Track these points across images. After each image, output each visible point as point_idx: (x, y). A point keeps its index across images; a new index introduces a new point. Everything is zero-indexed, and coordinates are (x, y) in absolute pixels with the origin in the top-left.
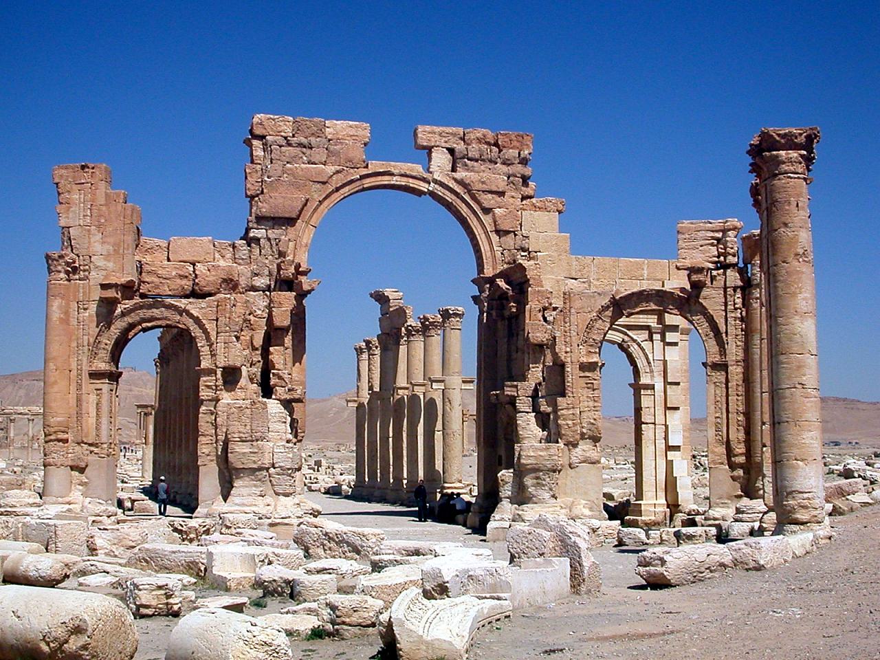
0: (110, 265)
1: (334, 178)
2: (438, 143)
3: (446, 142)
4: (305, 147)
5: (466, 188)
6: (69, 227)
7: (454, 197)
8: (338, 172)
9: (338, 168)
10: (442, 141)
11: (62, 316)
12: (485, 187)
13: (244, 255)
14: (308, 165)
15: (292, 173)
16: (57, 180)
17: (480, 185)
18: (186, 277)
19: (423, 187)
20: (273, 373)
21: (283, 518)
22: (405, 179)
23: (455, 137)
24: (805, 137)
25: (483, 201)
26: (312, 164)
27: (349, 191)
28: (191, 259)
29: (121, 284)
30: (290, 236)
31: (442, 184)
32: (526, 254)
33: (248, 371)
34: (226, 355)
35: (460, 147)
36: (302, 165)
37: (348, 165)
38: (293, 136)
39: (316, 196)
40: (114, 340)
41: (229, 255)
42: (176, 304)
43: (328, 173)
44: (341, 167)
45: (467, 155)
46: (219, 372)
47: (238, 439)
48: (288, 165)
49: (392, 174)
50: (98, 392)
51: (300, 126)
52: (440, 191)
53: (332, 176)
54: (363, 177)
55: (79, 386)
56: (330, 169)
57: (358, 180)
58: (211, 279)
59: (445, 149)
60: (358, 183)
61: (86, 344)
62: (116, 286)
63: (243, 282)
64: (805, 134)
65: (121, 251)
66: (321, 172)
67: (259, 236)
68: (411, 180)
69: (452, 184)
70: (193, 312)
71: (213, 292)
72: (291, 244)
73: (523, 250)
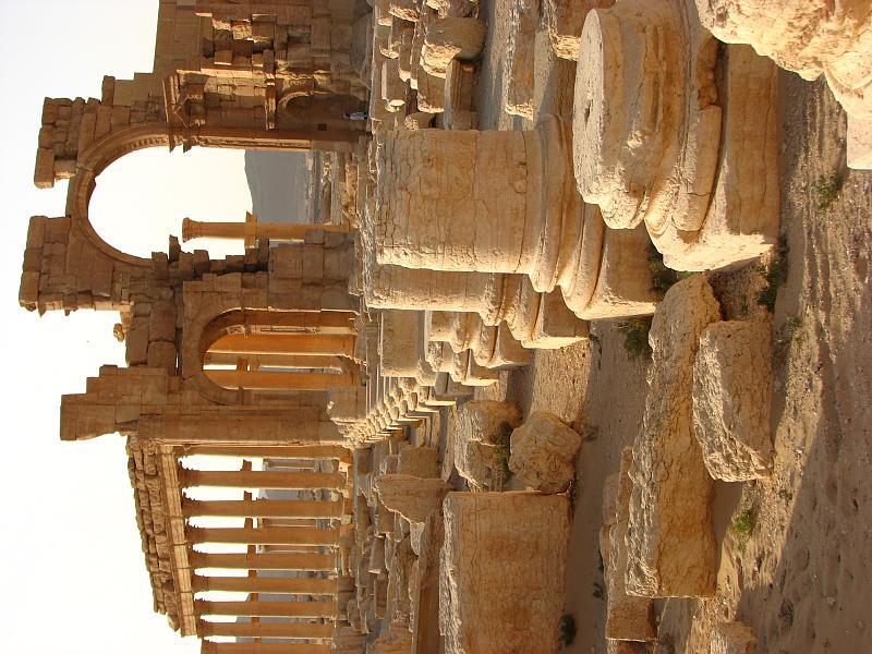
0: (150, 387)
8: (74, 235)
16: (73, 436)
28: (146, 343)
31: (87, 162)
32: (150, 105)
35: (58, 150)
41: (144, 319)
48: (67, 272)
52: (93, 163)
55: (253, 413)
56: (72, 240)
61: (217, 407)
67: (127, 294)
69: (87, 154)
72: (136, 269)
73: (146, 107)
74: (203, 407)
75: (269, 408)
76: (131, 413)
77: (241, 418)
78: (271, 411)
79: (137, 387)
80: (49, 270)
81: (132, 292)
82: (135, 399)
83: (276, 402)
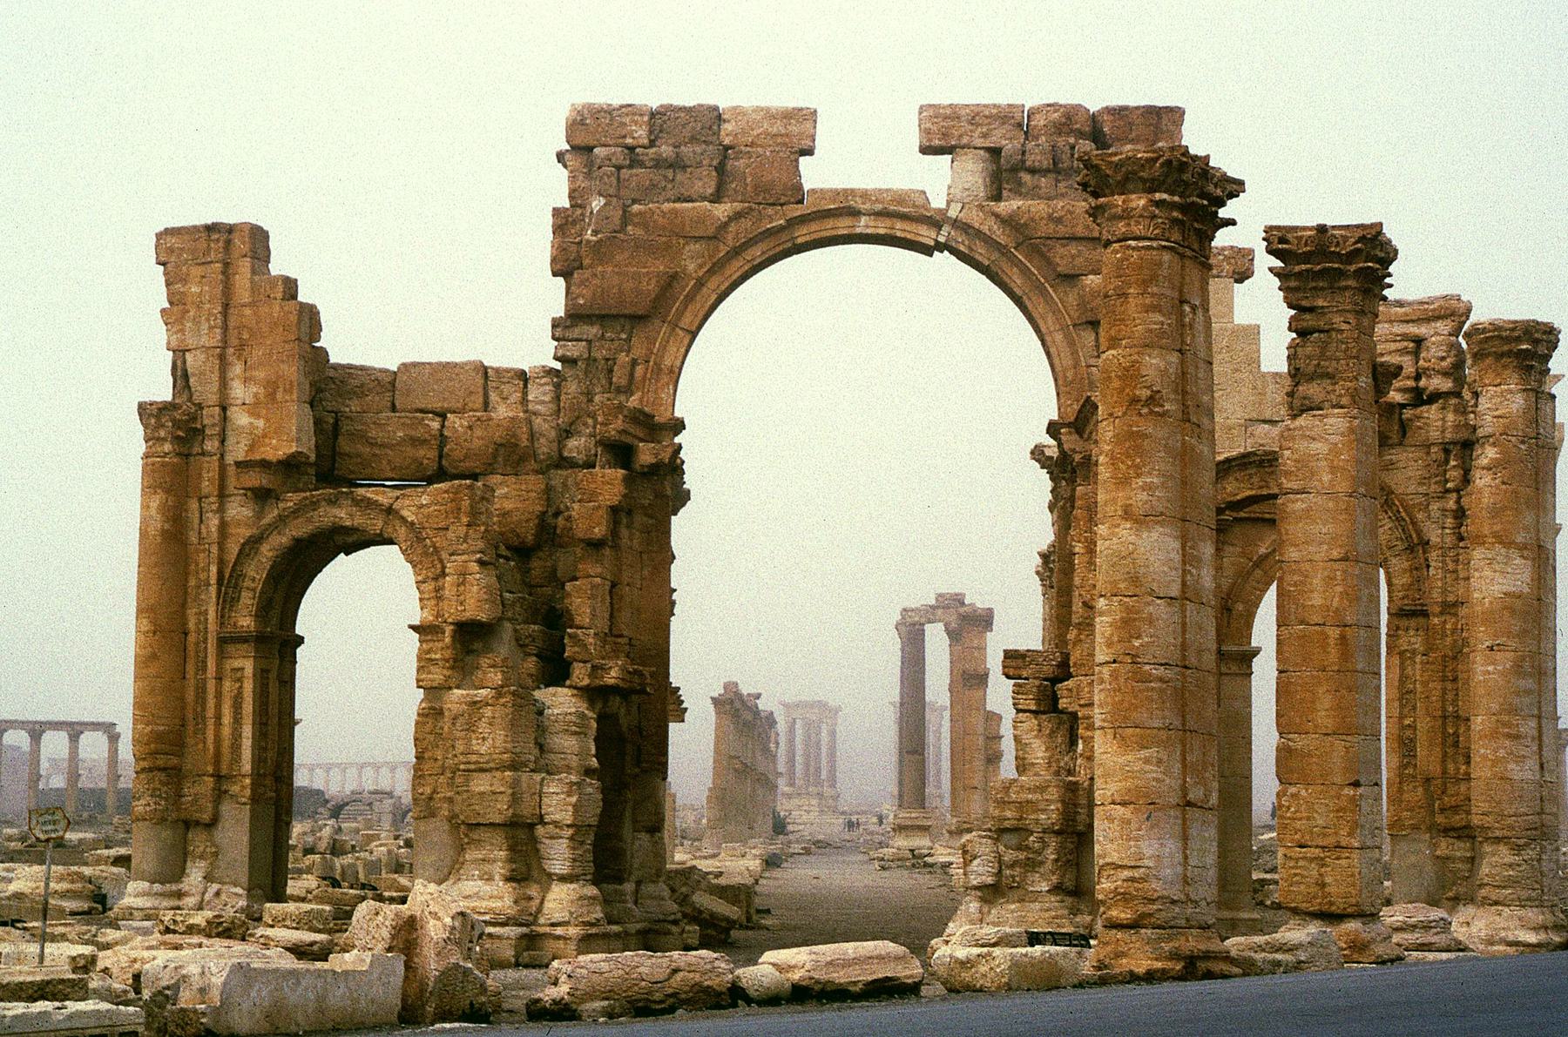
0: (261, 423)
1: (732, 228)
2: (965, 140)
3: (985, 136)
4: (670, 166)
5: (1017, 230)
6: (184, 351)
7: (995, 256)
8: (737, 216)
9: (738, 206)
10: (976, 135)
11: (167, 526)
12: (1062, 230)
13: (545, 394)
14: (677, 205)
15: (644, 221)
17: (1052, 226)
18: (424, 442)
19: (927, 235)
20: (570, 636)
21: (553, 925)
22: (888, 222)
23: (1004, 123)
24: (1162, 165)
25: (1058, 260)
26: (688, 201)
27: (763, 253)
28: (438, 405)
29: (279, 462)
30: (638, 351)
33: (516, 631)
34: (462, 598)
36: (667, 206)
37: (760, 199)
38: (652, 144)
39: (691, 267)
40: (266, 572)
42: (375, 497)
43: (719, 219)
44: (746, 205)
45: (1023, 162)
46: (449, 629)
47: (472, 767)
48: (636, 208)
49: (855, 213)
50: (239, 674)
51: (665, 122)
53: (726, 225)
54: (792, 223)
56: (722, 210)
57: (781, 229)
58: (477, 443)
59: (982, 152)
60: (784, 237)
62: (264, 464)
63: (544, 448)
64: (1161, 160)
65: (279, 396)
66: (701, 219)
68: (899, 225)
69: (990, 227)
70: (405, 513)
71: (478, 471)
74: (214, 549)
75: (211, 703)
76: (206, 391)
77: (192, 638)
78: (204, 710)
79: (262, 390)
80: (641, 164)
81: (580, 363)
82: (238, 391)
83: (227, 719)
